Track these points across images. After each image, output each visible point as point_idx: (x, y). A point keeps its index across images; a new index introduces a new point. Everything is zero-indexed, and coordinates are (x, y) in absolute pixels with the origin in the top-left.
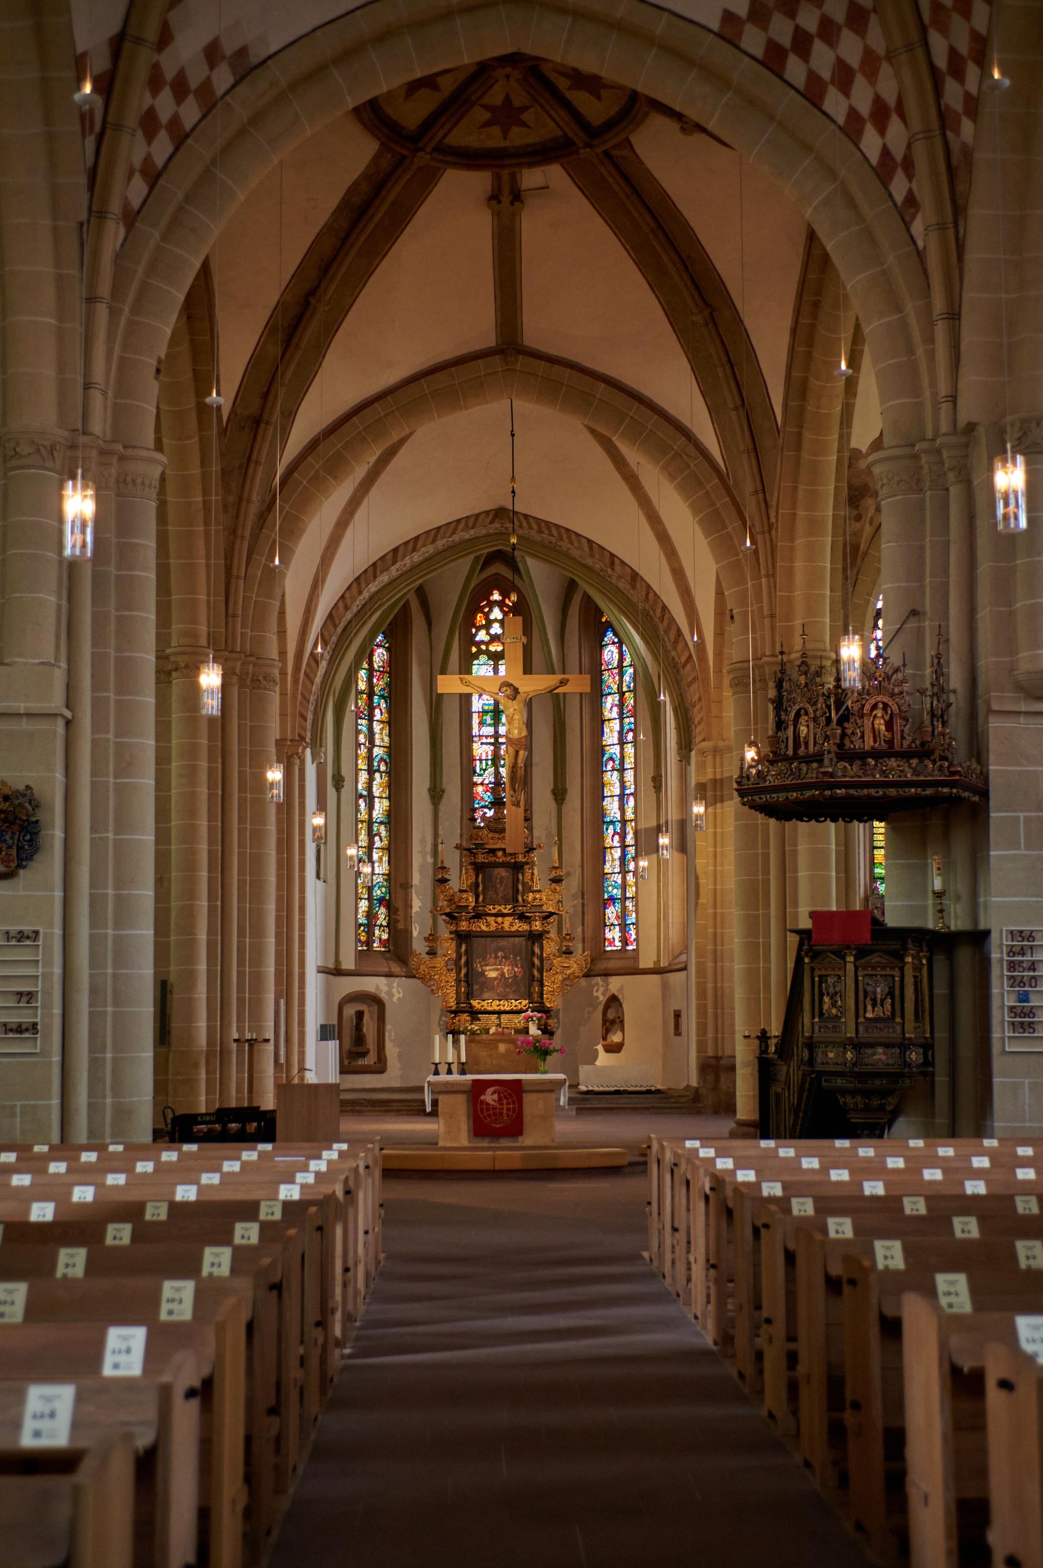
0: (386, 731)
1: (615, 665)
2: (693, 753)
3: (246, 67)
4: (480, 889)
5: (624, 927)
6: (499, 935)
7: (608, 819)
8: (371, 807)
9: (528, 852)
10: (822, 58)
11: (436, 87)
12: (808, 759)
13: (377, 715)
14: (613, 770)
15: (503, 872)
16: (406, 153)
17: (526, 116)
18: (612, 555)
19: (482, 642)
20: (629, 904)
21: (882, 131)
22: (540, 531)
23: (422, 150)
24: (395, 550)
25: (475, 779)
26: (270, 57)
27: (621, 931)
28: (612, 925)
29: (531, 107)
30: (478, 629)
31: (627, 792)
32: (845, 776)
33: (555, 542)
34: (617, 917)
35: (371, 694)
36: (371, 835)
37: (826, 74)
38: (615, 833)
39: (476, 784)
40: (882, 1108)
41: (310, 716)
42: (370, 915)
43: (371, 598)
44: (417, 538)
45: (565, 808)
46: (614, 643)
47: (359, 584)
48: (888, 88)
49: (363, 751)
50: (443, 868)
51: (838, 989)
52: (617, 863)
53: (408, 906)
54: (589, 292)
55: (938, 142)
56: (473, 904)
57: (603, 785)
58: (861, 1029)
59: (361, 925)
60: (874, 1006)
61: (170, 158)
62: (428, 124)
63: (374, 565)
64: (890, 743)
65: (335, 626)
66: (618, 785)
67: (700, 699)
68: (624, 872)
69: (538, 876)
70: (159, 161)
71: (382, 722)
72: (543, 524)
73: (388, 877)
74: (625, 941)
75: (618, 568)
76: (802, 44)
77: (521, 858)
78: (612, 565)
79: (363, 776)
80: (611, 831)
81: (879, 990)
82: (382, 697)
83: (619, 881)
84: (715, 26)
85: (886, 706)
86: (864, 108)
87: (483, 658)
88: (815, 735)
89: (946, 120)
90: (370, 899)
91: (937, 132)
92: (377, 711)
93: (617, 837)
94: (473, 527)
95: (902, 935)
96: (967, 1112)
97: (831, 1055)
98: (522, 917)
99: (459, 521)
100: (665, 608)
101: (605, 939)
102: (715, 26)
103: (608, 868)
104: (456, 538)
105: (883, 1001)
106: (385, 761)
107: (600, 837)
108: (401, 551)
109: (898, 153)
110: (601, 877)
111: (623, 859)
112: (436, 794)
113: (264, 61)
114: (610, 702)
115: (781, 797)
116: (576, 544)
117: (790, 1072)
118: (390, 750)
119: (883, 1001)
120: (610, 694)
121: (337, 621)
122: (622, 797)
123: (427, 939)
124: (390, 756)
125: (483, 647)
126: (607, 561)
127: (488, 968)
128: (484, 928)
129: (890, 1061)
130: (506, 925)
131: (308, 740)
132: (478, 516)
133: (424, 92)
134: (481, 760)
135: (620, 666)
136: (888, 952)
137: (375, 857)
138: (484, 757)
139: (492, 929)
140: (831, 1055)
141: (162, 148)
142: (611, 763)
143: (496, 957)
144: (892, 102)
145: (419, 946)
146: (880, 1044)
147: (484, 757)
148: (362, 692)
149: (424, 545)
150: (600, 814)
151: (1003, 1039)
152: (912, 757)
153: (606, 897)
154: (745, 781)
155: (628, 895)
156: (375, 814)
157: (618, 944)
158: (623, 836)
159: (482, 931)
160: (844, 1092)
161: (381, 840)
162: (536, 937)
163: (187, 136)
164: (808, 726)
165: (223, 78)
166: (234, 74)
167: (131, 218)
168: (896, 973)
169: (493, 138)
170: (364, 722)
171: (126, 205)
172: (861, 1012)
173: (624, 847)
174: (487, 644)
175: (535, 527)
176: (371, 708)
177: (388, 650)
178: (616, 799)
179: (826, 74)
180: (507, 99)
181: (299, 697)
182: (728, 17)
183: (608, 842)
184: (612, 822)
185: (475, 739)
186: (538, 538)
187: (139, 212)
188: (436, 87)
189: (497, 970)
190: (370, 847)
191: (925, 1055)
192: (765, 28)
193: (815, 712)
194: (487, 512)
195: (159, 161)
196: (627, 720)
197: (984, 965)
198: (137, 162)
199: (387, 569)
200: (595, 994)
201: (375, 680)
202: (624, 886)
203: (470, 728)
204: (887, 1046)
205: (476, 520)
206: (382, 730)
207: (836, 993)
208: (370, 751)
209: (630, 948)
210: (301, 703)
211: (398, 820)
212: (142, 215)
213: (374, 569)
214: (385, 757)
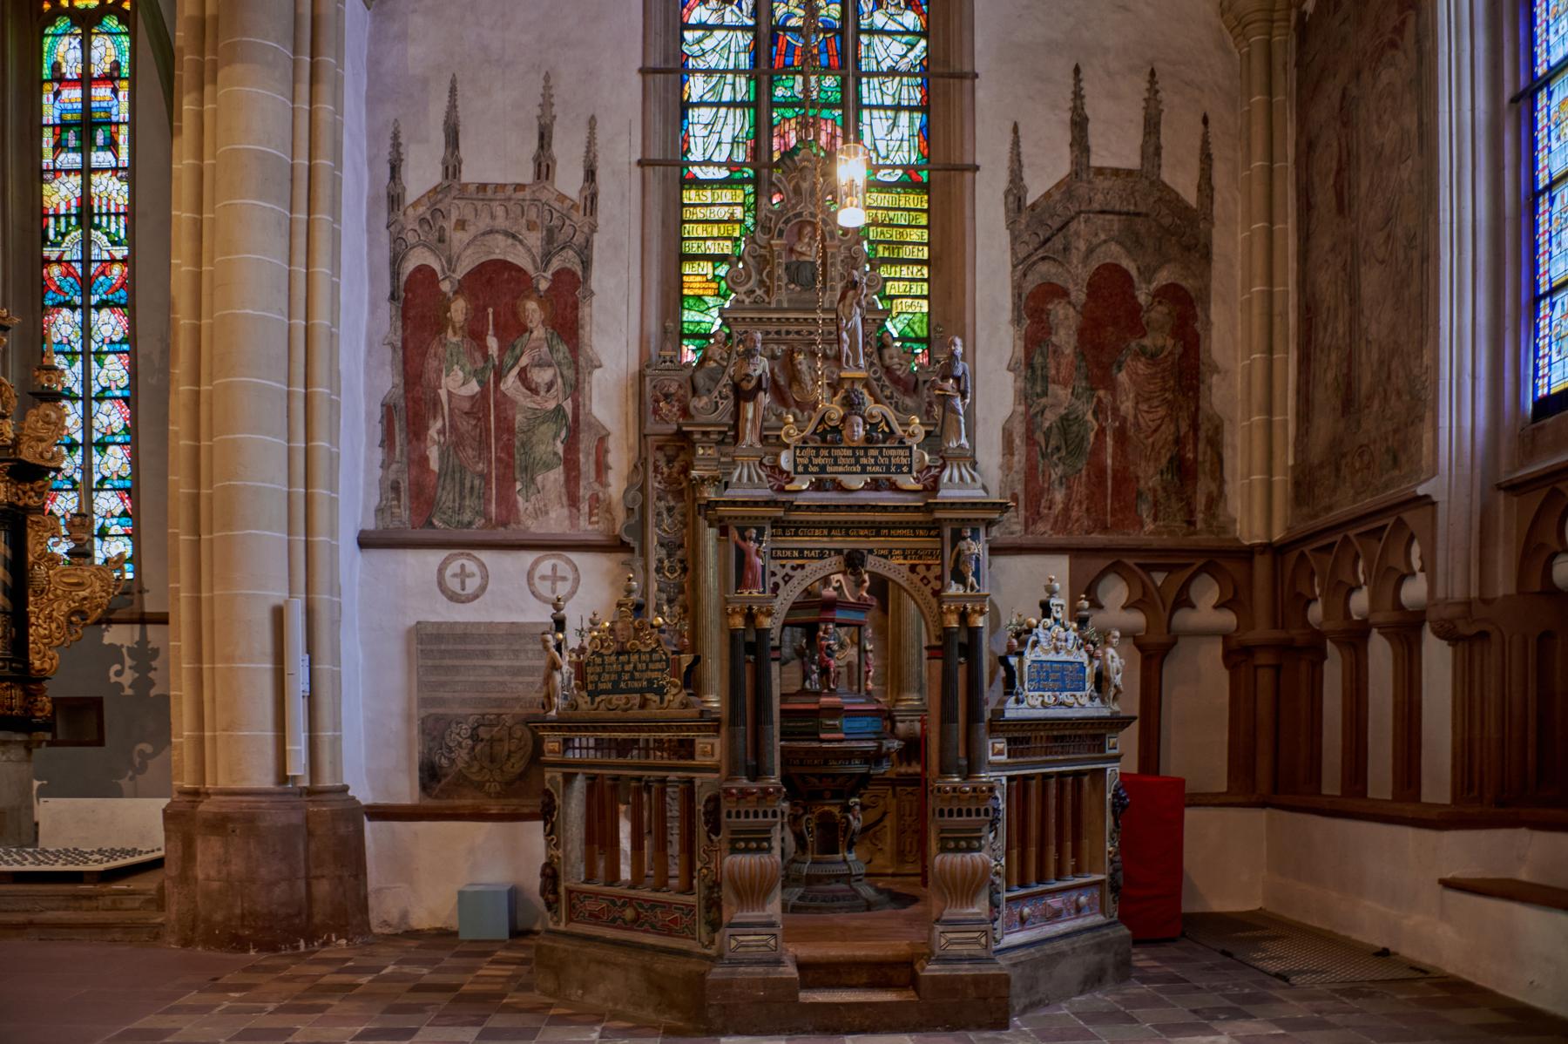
39: (47, 262)
87: (63, 24)
134: (57, 216)
138: (62, 211)
147: (62, 211)
185: (49, 176)
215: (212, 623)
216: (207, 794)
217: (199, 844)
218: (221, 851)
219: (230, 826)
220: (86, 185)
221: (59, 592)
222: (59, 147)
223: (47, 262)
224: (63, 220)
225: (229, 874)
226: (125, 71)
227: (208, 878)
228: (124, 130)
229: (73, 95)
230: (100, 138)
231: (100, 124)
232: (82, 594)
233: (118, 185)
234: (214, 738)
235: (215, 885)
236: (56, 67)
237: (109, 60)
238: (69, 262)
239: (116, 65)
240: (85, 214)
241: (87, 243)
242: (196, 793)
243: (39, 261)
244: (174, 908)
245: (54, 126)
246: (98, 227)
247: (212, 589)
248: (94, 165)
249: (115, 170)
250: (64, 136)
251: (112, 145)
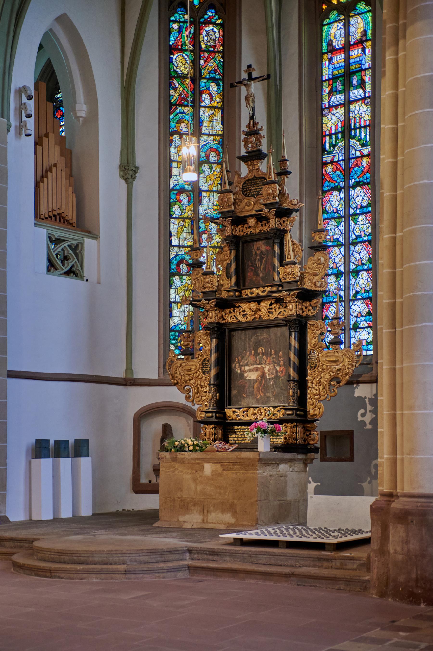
35: (196, 79)
39: (325, 164)
71: (214, 108)
82: (214, 80)
87: (333, 15)
92: (205, 97)
106: (216, 151)
127: (247, 368)
128: (241, 318)
134: (330, 135)
138: (334, 131)
139: (250, 319)
143: (256, 354)
148: (183, 77)
156: (202, 210)
162: (300, 325)
176: (197, 93)
189: (257, 370)
201: (202, 62)
214: (216, 146)
215: (402, 384)
216: (397, 497)
217: (391, 530)
218: (404, 535)
219: (410, 518)
220: (348, 112)
221: (325, 367)
222: (331, 93)
223: (325, 164)
224: (334, 136)
225: (408, 551)
226: (369, 36)
227: (396, 552)
228: (369, 72)
229: (340, 58)
230: (355, 80)
231: (355, 72)
232: (338, 367)
233: (365, 108)
234: (402, 460)
235: (400, 557)
236: (330, 43)
237: (359, 31)
238: (337, 162)
239: (365, 32)
240: (347, 131)
241: (348, 148)
242: (391, 495)
243: (320, 164)
244: (375, 571)
245: (329, 80)
246: (354, 137)
247: (402, 363)
248: (352, 99)
249: (363, 99)
250: (335, 84)
251: (362, 84)
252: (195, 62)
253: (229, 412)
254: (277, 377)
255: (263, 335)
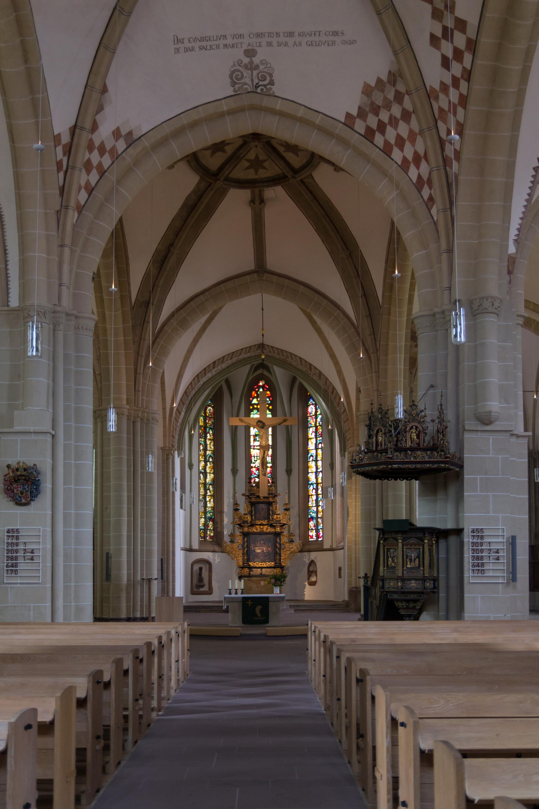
0: (212, 444)
1: (314, 413)
2: (346, 453)
3: (131, 140)
4: (253, 513)
5: (317, 531)
6: (262, 533)
7: (310, 483)
8: (205, 477)
9: (274, 497)
10: (391, 134)
11: (224, 151)
12: (381, 452)
13: (209, 437)
14: (313, 460)
15: (263, 506)
16: (211, 181)
17: (264, 164)
18: (311, 365)
19: (255, 404)
20: (320, 520)
21: (418, 167)
22: (278, 354)
23: (219, 180)
24: (214, 363)
25: (252, 465)
26: (142, 136)
27: (316, 532)
28: (312, 529)
29: (267, 160)
30: (253, 399)
31: (319, 470)
32: (397, 459)
33: (286, 359)
34: (314, 526)
35: (205, 427)
36: (206, 490)
37: (393, 141)
38: (314, 489)
39: (252, 467)
40: (414, 608)
41: (177, 437)
42: (206, 525)
43: (204, 384)
44: (224, 357)
45: (292, 477)
46: (313, 404)
47: (198, 378)
48: (420, 147)
49: (202, 452)
50: (237, 504)
51: (395, 554)
52: (314, 502)
53: (222, 521)
54: (297, 248)
55: (443, 171)
56: (250, 520)
57: (308, 468)
58: (405, 572)
59: (201, 529)
60: (411, 562)
61: (98, 182)
62: (221, 168)
63: (205, 369)
64: (418, 444)
65: (188, 397)
66: (315, 467)
67: (349, 429)
68: (317, 506)
69: (279, 508)
70: (93, 183)
72: (280, 351)
73: (213, 508)
74: (318, 536)
75: (313, 370)
76: (382, 127)
77: (271, 500)
78: (311, 369)
79: (202, 464)
80: (311, 488)
81: (413, 555)
83: (315, 510)
84: (343, 120)
85: (417, 427)
86: (410, 157)
87: (255, 411)
88: (385, 440)
89: (446, 162)
90: (205, 518)
91: (442, 167)
92: (208, 435)
93: (314, 491)
94: (249, 352)
95: (423, 530)
96: (455, 611)
97: (392, 584)
98: (271, 526)
99: (242, 349)
100: (334, 388)
101: (309, 535)
102: (343, 120)
103: (310, 504)
104: (241, 357)
105: (415, 560)
107: (307, 491)
108: (217, 363)
109: (425, 177)
110: (308, 508)
111: (317, 501)
112: (234, 471)
113: (140, 137)
114: (311, 431)
115: (370, 468)
116: (294, 359)
117: (377, 592)
118: (214, 452)
119: (415, 560)
120: (311, 427)
121: (188, 394)
122: (316, 473)
123: (229, 536)
124: (214, 455)
125: (255, 406)
126: (308, 366)
128: (255, 531)
129: (418, 587)
130: (265, 530)
131: (176, 447)
132: (251, 347)
133: (219, 154)
134: (254, 457)
135: (316, 415)
136: (417, 538)
137: (208, 499)
139: (259, 531)
140: (392, 584)
141: (94, 177)
142: (312, 458)
143: (260, 543)
144: (422, 154)
145: (227, 539)
146: (413, 579)
147: (256, 455)
148: (202, 426)
149: (227, 360)
150: (308, 480)
151: (469, 577)
152: (428, 450)
153: (309, 517)
154: (354, 462)
155: (319, 516)
156: (208, 480)
157: (314, 537)
158: (317, 490)
159: (254, 532)
160: (398, 600)
161: (210, 492)
162: (278, 535)
163: (105, 171)
164: (382, 437)
165: (121, 145)
166: (126, 143)
167: (80, 209)
168: (421, 547)
169: (251, 175)
170: (202, 440)
171: (78, 203)
172: (405, 565)
173: (317, 495)
174: (257, 405)
175: (276, 352)
177: (213, 407)
178: (314, 473)
179: (393, 141)
180: (257, 157)
181: (172, 428)
182: (348, 115)
183: (310, 493)
184: (312, 484)
186: (277, 357)
187: (84, 206)
188: (224, 151)
189: (260, 549)
190: (205, 496)
191: (434, 584)
192: (365, 121)
193: (385, 430)
194: (255, 345)
195: (93, 183)
196: (319, 439)
197: (461, 544)
198: (83, 183)
199: (211, 371)
200: (304, 560)
202: (317, 512)
203: (250, 442)
204: (416, 580)
205: (250, 349)
206: (210, 443)
207: (394, 556)
208: (205, 453)
209: (320, 539)
210: (173, 431)
211: (218, 483)
212: (85, 208)
213: (205, 371)
223: (252, 467)
232: (292, 550)
252: (205, 420)
253: (251, 564)
254: (268, 552)
255: (263, 537)
